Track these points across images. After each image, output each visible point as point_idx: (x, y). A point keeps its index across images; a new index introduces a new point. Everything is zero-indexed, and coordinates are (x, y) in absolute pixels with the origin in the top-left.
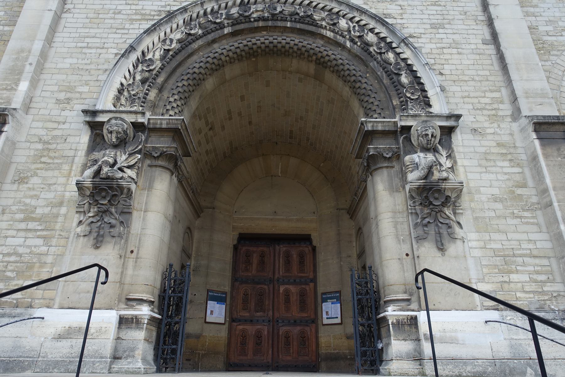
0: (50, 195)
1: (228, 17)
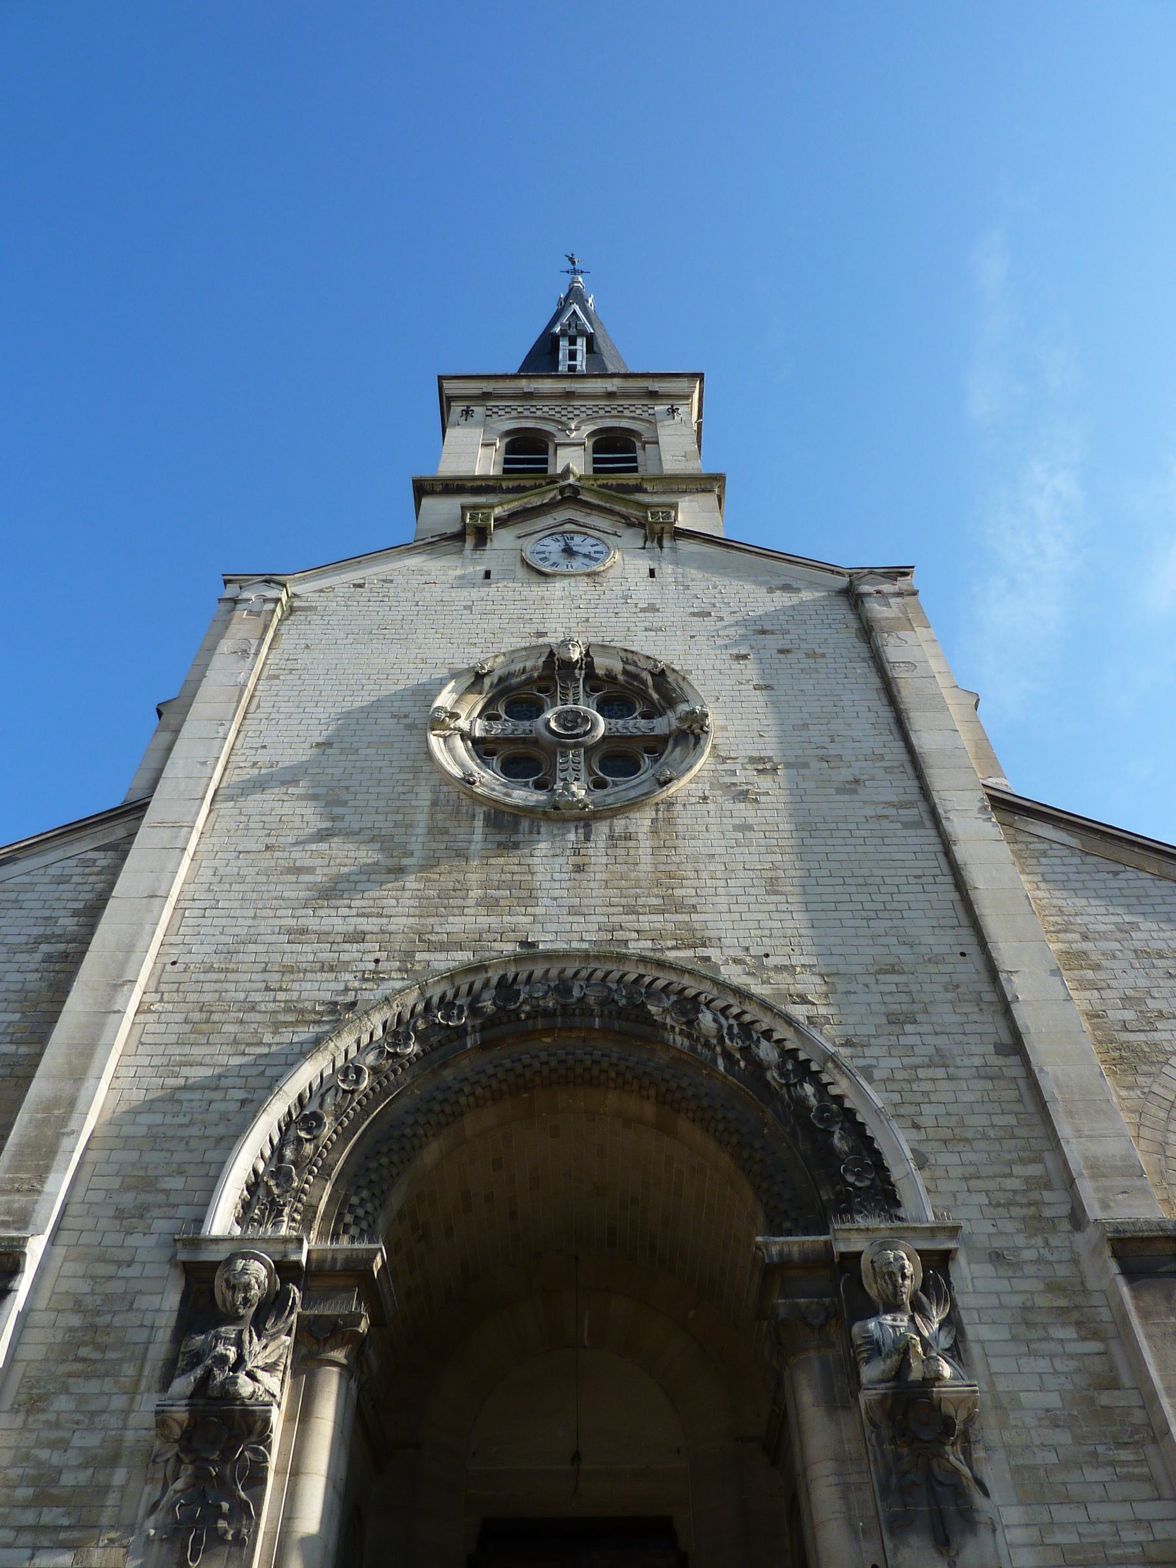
0: (91, 1440)
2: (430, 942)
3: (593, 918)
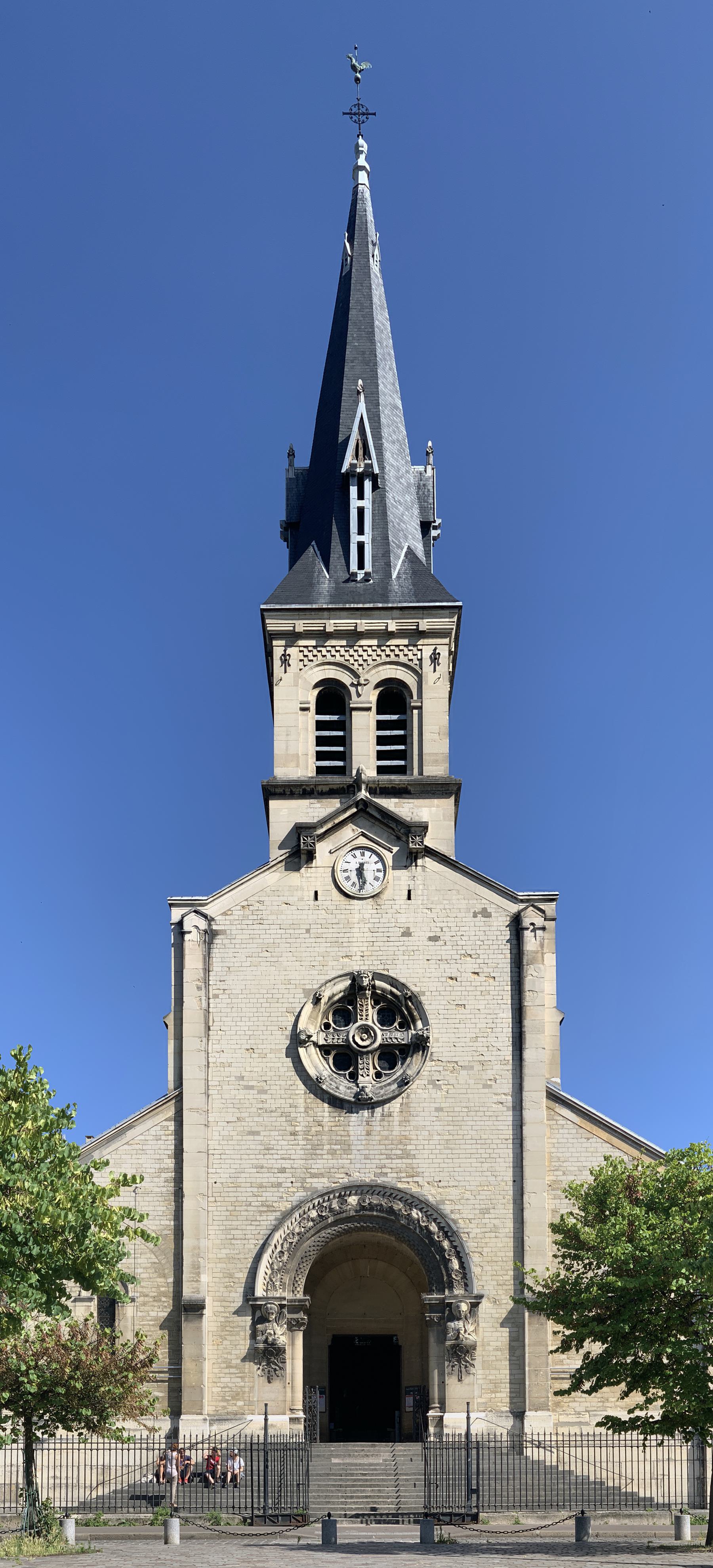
1: (331, 1210)
2: (310, 1173)
3: (373, 1161)
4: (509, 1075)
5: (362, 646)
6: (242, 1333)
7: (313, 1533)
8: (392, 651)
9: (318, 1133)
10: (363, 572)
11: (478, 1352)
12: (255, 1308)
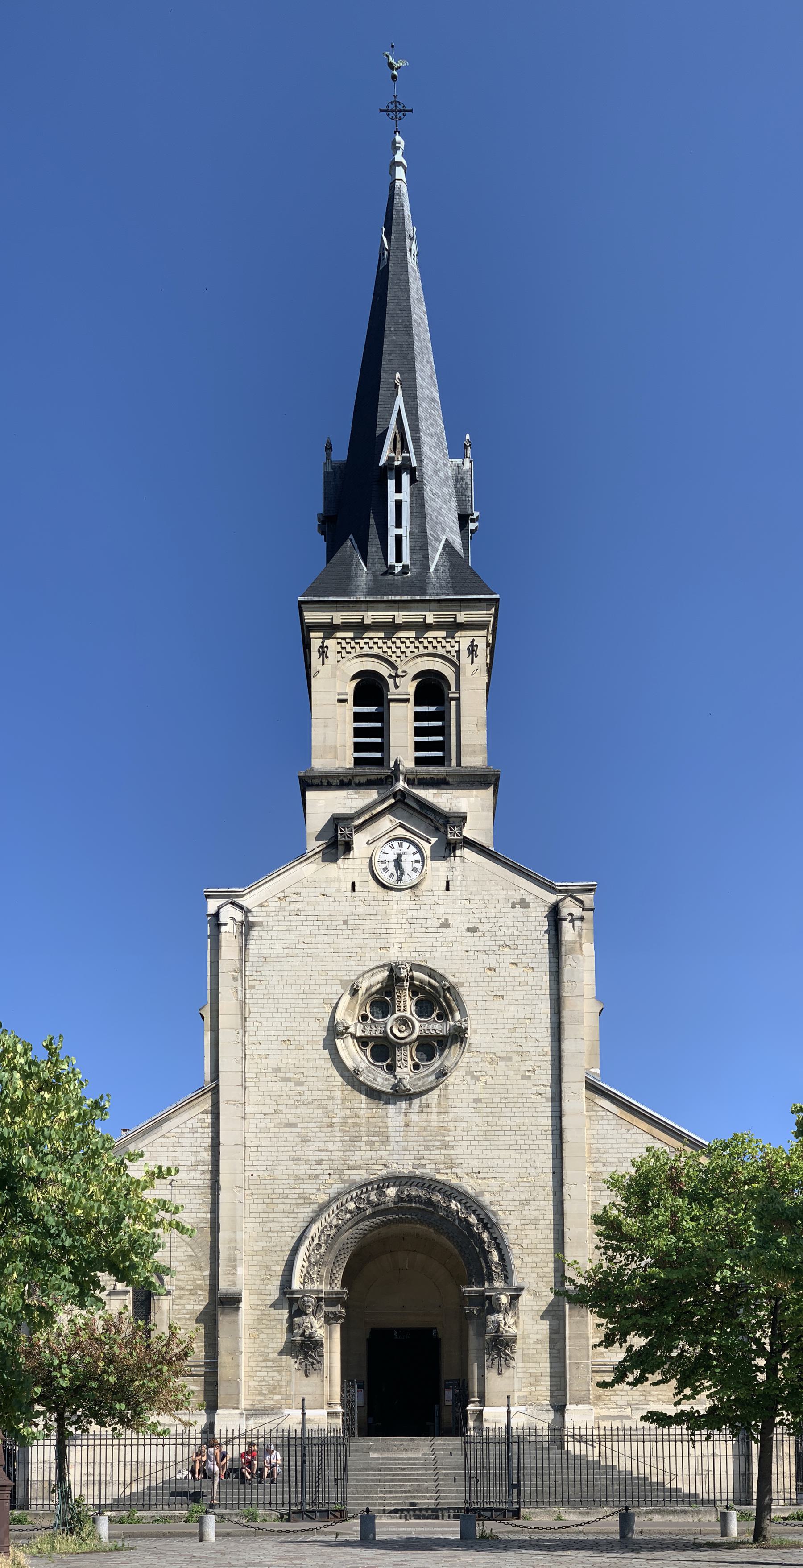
1: (369, 1202)
2: (348, 1165)
4: (548, 1066)
5: (400, 638)
6: (279, 1326)
7: (351, 1530)
8: (429, 642)
9: (355, 1125)
10: (401, 564)
11: (519, 1345)
12: (292, 1301)
